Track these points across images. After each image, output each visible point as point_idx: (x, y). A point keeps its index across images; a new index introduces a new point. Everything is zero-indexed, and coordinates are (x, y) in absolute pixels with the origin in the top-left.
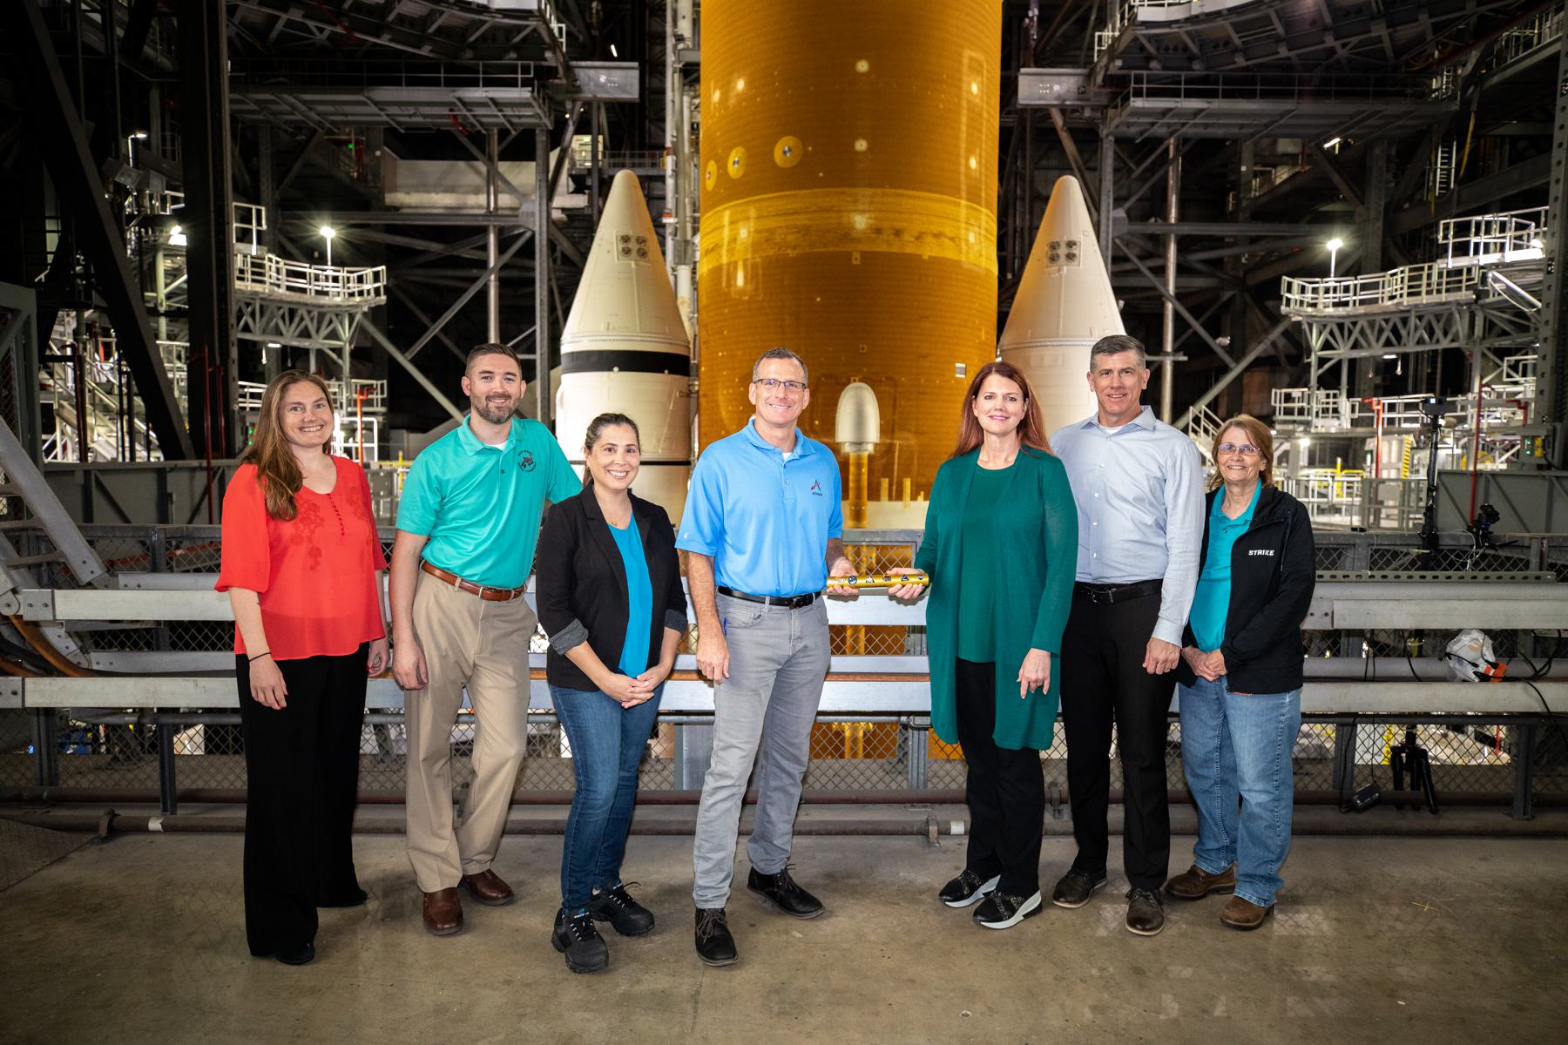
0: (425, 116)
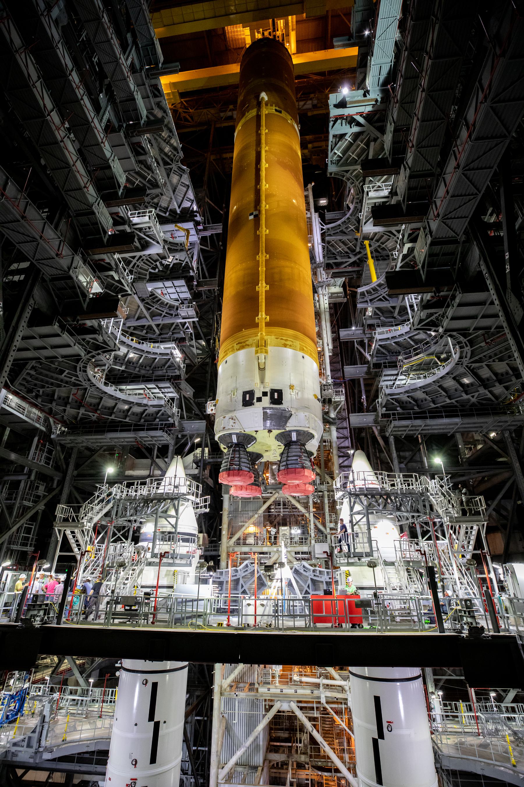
0: (127, 442)
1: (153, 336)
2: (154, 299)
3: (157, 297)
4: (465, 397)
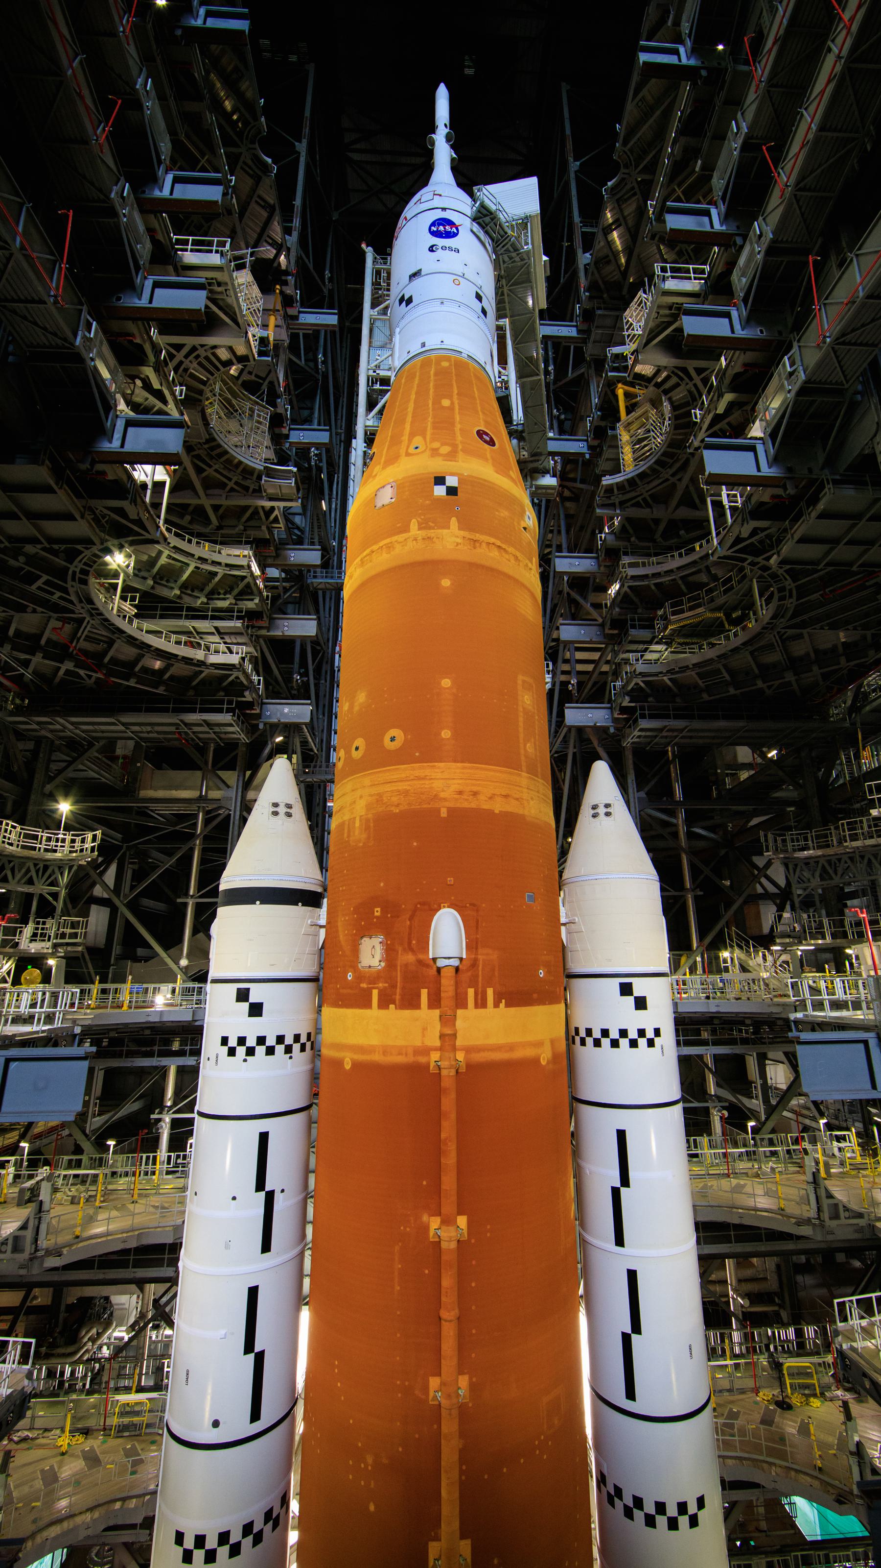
0: (158, 732)
1: (202, 530)
2: (212, 449)
3: (219, 446)
4: (760, 684)
